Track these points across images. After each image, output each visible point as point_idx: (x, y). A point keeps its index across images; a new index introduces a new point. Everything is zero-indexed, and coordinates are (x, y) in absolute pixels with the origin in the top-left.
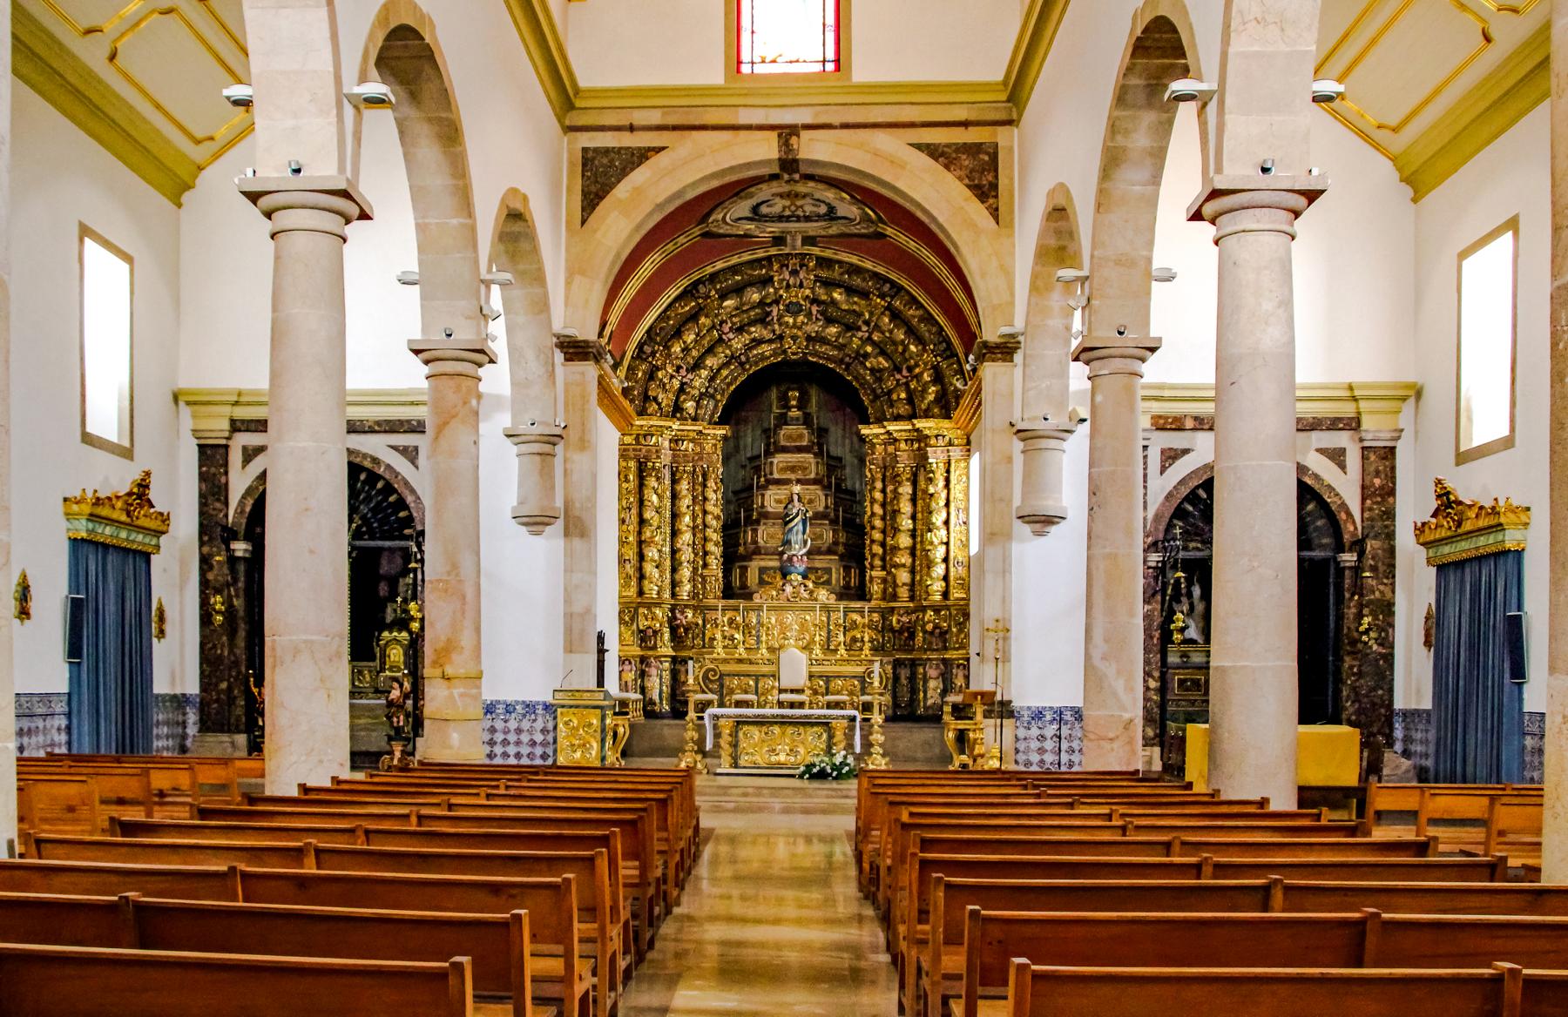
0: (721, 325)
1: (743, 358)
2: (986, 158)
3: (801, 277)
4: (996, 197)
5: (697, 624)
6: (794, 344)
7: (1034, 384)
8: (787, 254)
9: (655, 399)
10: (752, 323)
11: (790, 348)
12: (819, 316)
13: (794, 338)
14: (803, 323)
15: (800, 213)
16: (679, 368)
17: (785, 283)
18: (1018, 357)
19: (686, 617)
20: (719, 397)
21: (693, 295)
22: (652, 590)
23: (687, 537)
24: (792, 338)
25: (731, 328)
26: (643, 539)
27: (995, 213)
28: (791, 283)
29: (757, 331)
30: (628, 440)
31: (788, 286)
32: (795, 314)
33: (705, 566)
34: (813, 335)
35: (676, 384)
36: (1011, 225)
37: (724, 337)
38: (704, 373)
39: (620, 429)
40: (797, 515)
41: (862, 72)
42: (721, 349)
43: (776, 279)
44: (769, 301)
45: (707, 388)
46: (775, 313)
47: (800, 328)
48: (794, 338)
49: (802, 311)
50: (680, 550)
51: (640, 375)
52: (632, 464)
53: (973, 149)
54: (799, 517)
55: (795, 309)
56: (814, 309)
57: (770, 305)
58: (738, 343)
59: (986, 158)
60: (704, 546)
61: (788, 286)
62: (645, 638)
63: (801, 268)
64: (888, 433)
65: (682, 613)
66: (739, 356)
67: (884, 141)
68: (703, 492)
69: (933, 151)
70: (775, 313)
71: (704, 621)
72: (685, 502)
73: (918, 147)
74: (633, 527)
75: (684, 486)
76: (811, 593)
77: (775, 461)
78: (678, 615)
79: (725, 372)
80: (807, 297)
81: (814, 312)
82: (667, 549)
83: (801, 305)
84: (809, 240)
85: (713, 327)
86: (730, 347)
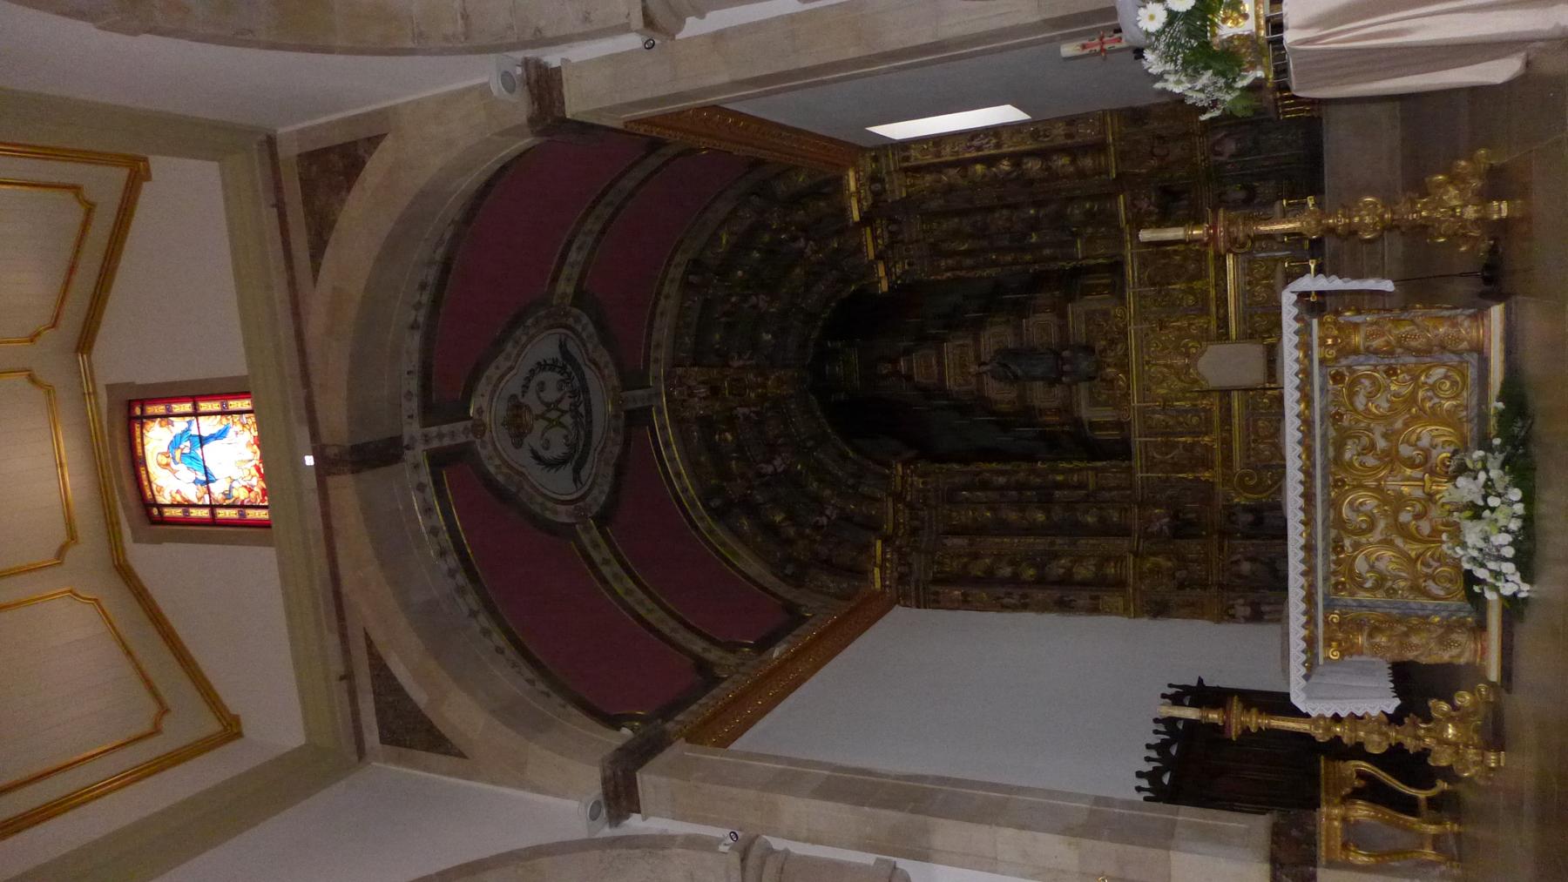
2: (314, 168)
3: (694, 384)
4: (355, 143)
15: (565, 405)
18: (553, 58)
27: (374, 141)
36: (382, 114)
41: (234, 365)
46: (746, 410)
53: (308, 186)
59: (314, 168)
64: (879, 257)
67: (315, 326)
69: (318, 250)
73: (316, 270)
84: (632, 377)
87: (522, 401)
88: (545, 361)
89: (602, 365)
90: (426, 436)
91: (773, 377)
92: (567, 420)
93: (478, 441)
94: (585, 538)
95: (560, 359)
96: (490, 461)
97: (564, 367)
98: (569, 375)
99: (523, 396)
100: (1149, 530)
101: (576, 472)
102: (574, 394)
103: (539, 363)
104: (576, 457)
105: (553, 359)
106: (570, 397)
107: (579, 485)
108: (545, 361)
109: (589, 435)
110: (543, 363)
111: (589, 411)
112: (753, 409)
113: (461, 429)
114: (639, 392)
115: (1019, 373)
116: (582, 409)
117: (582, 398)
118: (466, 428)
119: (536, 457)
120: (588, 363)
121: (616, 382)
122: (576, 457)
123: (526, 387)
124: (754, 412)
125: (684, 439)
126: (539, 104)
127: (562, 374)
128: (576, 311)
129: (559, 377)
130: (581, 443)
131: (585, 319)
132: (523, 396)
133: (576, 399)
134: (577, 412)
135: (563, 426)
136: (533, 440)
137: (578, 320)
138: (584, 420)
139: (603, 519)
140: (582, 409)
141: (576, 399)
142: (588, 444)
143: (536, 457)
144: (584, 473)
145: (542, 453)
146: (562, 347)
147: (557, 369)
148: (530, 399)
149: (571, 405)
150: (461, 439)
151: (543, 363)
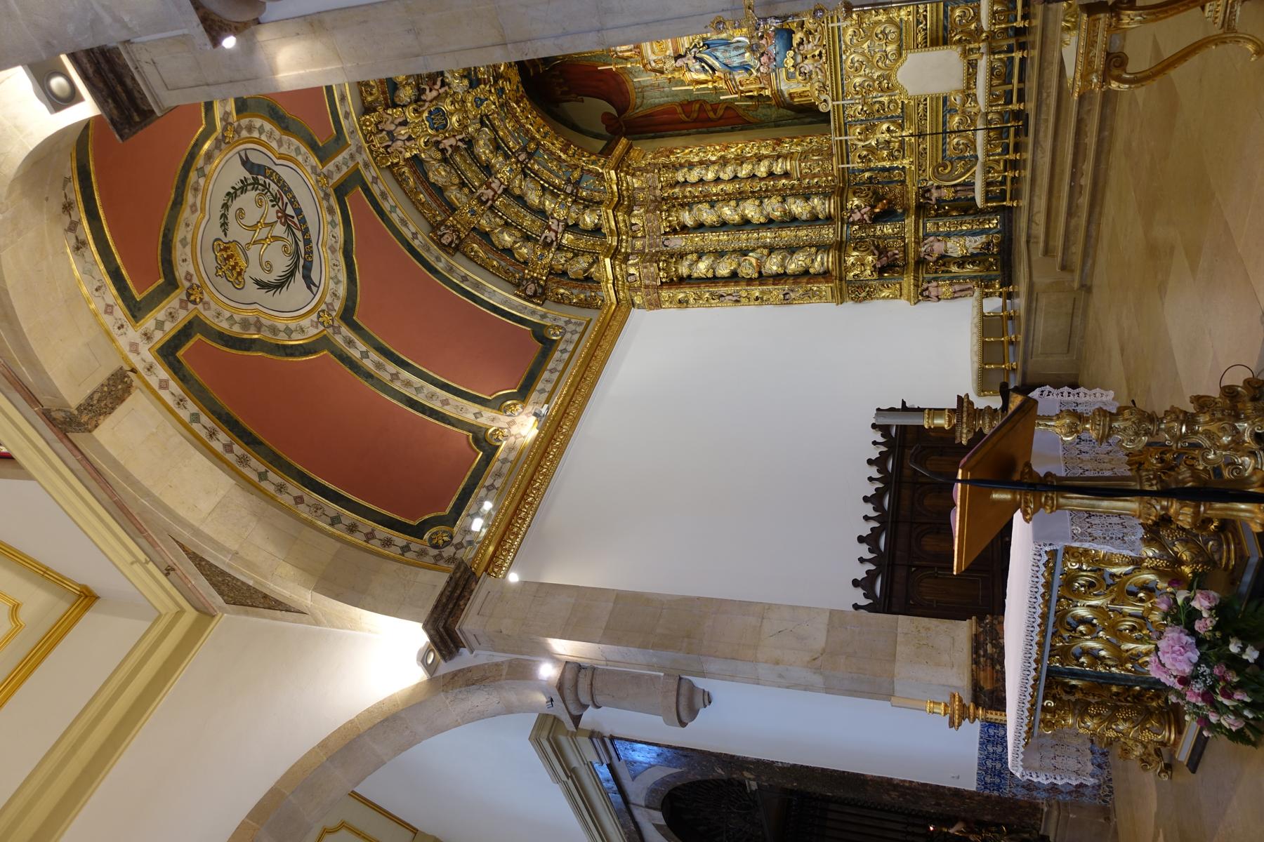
0: (485, 203)
1: (522, 157)
3: (392, 127)
5: (870, 178)
6: (487, 99)
7: (108, 20)
8: (371, 152)
9: (585, 271)
10: (476, 158)
11: (494, 104)
12: (437, 87)
13: (478, 102)
14: (452, 103)
15: (272, 215)
16: (547, 245)
17: (408, 144)
19: (858, 207)
20: (576, 174)
21: (457, 246)
22: (821, 262)
23: (751, 210)
24: (478, 107)
25: (489, 187)
26: (756, 275)
28: (406, 137)
29: (483, 150)
30: (638, 300)
31: (410, 138)
32: (445, 116)
33: (786, 175)
34: (466, 82)
35: (568, 239)
37: (499, 192)
38: (549, 205)
39: (629, 311)
40: (701, 60)
42: (517, 192)
43: (408, 155)
44: (439, 156)
45: (567, 195)
47: (463, 101)
48: (478, 102)
49: (438, 110)
50: (767, 216)
51: (562, 291)
52: (665, 294)
54: (706, 57)
55: (439, 120)
56: (430, 95)
57: (443, 151)
58: (505, 171)
60: (762, 179)
61: (410, 138)
62: (888, 268)
63: (382, 130)
65: (852, 211)
66: (522, 163)
68: (693, 184)
70: (452, 141)
71: (863, 171)
72: (708, 216)
74: (742, 290)
75: (687, 218)
76: (809, 33)
77: (652, 57)
78: (857, 216)
79: (546, 174)
80: (415, 110)
81: (434, 93)
82: (768, 236)
83: (430, 113)
85: (492, 208)
86: (510, 181)
87: (226, 240)
88: (233, 188)
89: (293, 154)
90: (145, 334)
91: (470, 98)
92: (280, 230)
93: (200, 306)
94: (339, 340)
95: (248, 176)
96: (221, 318)
97: (256, 181)
98: (264, 185)
99: (226, 235)
100: (851, 219)
101: (307, 278)
102: (275, 200)
103: (229, 194)
104: (302, 262)
105: (242, 181)
106: (273, 206)
107: (314, 289)
108: (233, 188)
109: (305, 232)
110: (232, 191)
111: (298, 211)
112: (458, 137)
113: (177, 306)
114: (339, 159)
115: (716, 64)
116: (290, 211)
117: (285, 200)
118: (181, 301)
119: (262, 285)
120: (278, 162)
121: (314, 160)
122: (302, 262)
123: (224, 225)
124: (460, 140)
125: (400, 180)
126: (115, 101)
127: (257, 189)
128: (244, 122)
129: (254, 193)
130: (301, 245)
131: (258, 122)
132: (226, 235)
133: (280, 204)
134: (286, 216)
135: (276, 238)
136: (254, 271)
137: (250, 128)
138: (294, 220)
139: (347, 315)
140: (290, 211)
141: (280, 204)
142: (307, 242)
143: (262, 285)
144: (315, 276)
145: (266, 278)
146: (246, 163)
147: (250, 188)
148: (237, 233)
149: (277, 212)
150: (183, 316)
151: (232, 191)
